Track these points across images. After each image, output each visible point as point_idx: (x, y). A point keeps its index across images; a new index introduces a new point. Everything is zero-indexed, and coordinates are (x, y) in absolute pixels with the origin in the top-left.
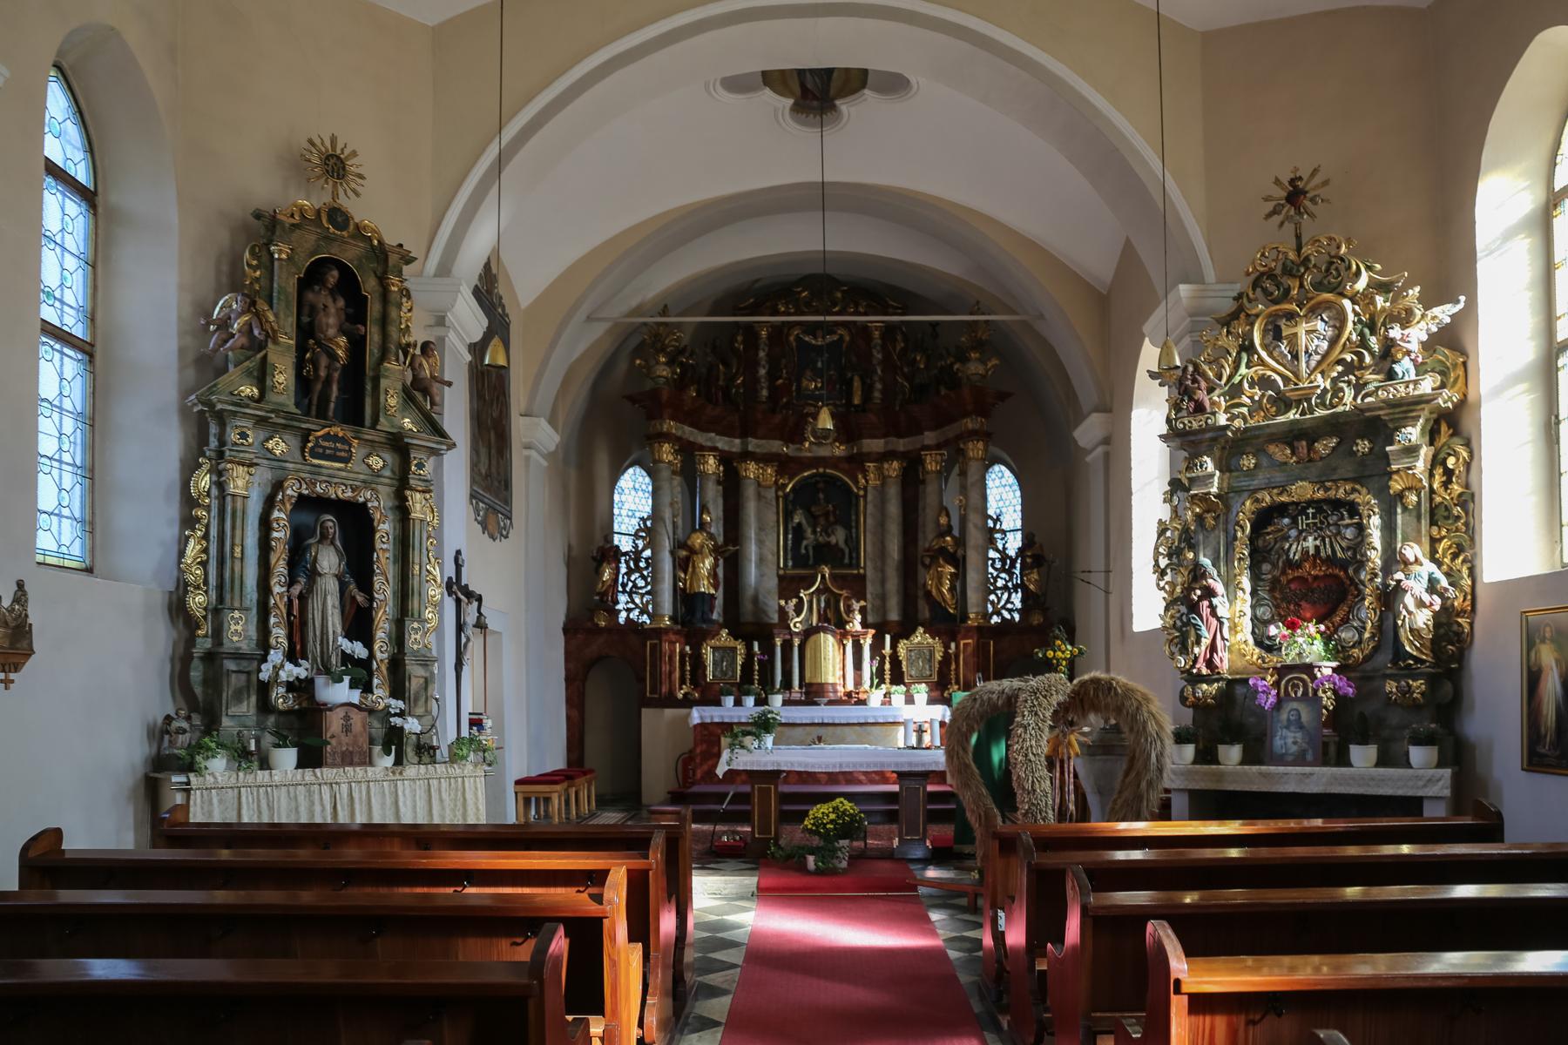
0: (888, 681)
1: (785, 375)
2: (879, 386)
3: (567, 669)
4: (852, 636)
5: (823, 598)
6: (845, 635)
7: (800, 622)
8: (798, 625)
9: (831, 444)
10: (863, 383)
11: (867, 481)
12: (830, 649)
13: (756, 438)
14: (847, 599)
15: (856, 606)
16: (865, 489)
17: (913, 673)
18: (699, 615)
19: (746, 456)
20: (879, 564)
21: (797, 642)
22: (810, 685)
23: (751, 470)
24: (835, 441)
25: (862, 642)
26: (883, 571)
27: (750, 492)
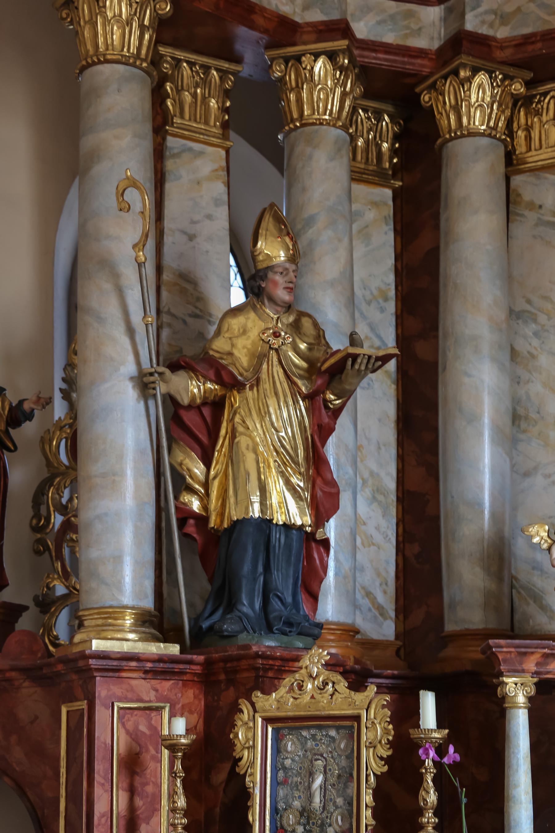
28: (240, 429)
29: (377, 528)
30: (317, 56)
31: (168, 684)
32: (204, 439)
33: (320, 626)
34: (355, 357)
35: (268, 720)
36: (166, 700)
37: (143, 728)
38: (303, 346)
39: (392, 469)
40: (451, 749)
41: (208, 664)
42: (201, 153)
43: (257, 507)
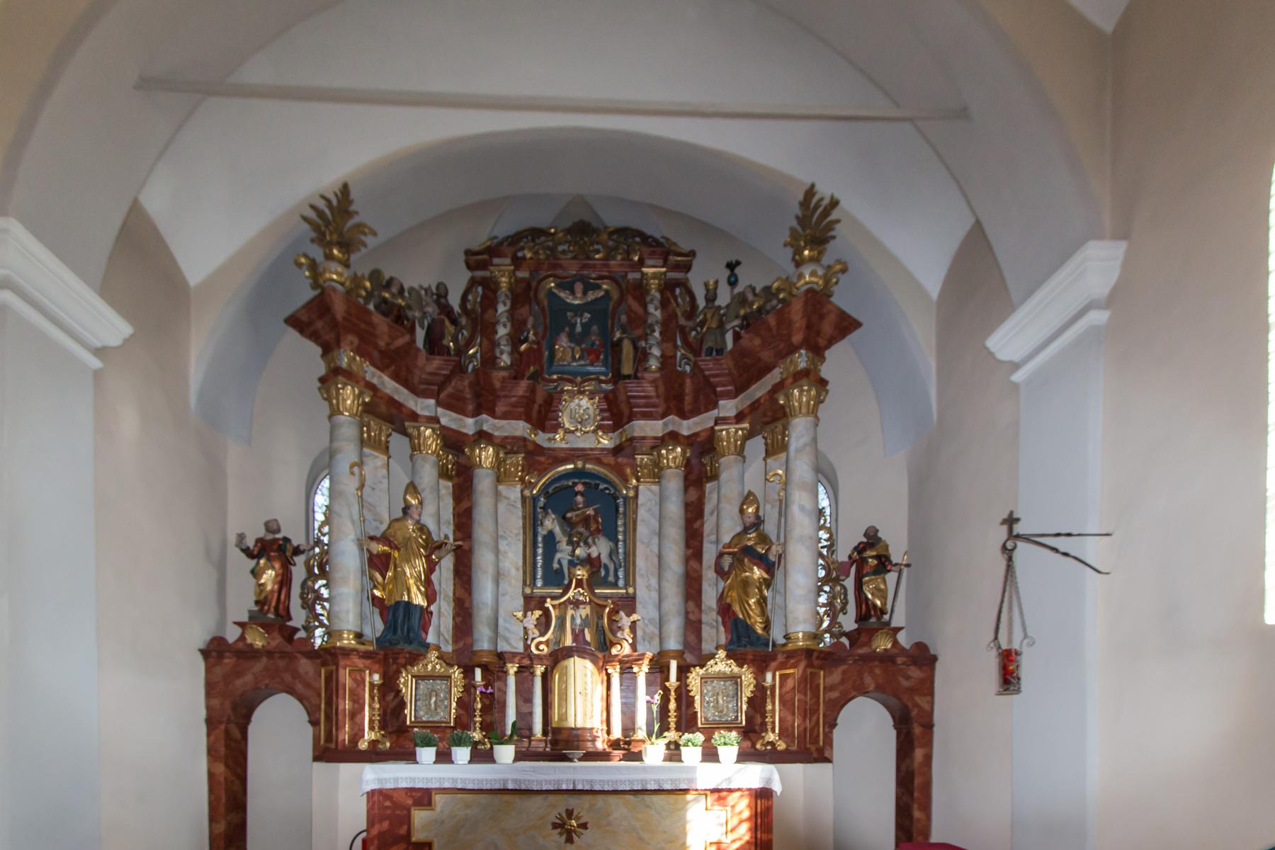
0: (673, 725)
1: (531, 337)
2: (656, 352)
3: (208, 708)
4: (621, 662)
6: (609, 659)
7: (547, 643)
10: (636, 348)
11: (638, 480)
16: (636, 489)
19: (483, 437)
22: (558, 731)
27: (484, 482)
29: (446, 610)
33: (429, 644)
34: (446, 544)
35: (413, 676)
36: (368, 668)
37: (358, 678)
38: (424, 537)
39: (452, 588)
40: (490, 688)
42: (376, 457)
43: (406, 597)
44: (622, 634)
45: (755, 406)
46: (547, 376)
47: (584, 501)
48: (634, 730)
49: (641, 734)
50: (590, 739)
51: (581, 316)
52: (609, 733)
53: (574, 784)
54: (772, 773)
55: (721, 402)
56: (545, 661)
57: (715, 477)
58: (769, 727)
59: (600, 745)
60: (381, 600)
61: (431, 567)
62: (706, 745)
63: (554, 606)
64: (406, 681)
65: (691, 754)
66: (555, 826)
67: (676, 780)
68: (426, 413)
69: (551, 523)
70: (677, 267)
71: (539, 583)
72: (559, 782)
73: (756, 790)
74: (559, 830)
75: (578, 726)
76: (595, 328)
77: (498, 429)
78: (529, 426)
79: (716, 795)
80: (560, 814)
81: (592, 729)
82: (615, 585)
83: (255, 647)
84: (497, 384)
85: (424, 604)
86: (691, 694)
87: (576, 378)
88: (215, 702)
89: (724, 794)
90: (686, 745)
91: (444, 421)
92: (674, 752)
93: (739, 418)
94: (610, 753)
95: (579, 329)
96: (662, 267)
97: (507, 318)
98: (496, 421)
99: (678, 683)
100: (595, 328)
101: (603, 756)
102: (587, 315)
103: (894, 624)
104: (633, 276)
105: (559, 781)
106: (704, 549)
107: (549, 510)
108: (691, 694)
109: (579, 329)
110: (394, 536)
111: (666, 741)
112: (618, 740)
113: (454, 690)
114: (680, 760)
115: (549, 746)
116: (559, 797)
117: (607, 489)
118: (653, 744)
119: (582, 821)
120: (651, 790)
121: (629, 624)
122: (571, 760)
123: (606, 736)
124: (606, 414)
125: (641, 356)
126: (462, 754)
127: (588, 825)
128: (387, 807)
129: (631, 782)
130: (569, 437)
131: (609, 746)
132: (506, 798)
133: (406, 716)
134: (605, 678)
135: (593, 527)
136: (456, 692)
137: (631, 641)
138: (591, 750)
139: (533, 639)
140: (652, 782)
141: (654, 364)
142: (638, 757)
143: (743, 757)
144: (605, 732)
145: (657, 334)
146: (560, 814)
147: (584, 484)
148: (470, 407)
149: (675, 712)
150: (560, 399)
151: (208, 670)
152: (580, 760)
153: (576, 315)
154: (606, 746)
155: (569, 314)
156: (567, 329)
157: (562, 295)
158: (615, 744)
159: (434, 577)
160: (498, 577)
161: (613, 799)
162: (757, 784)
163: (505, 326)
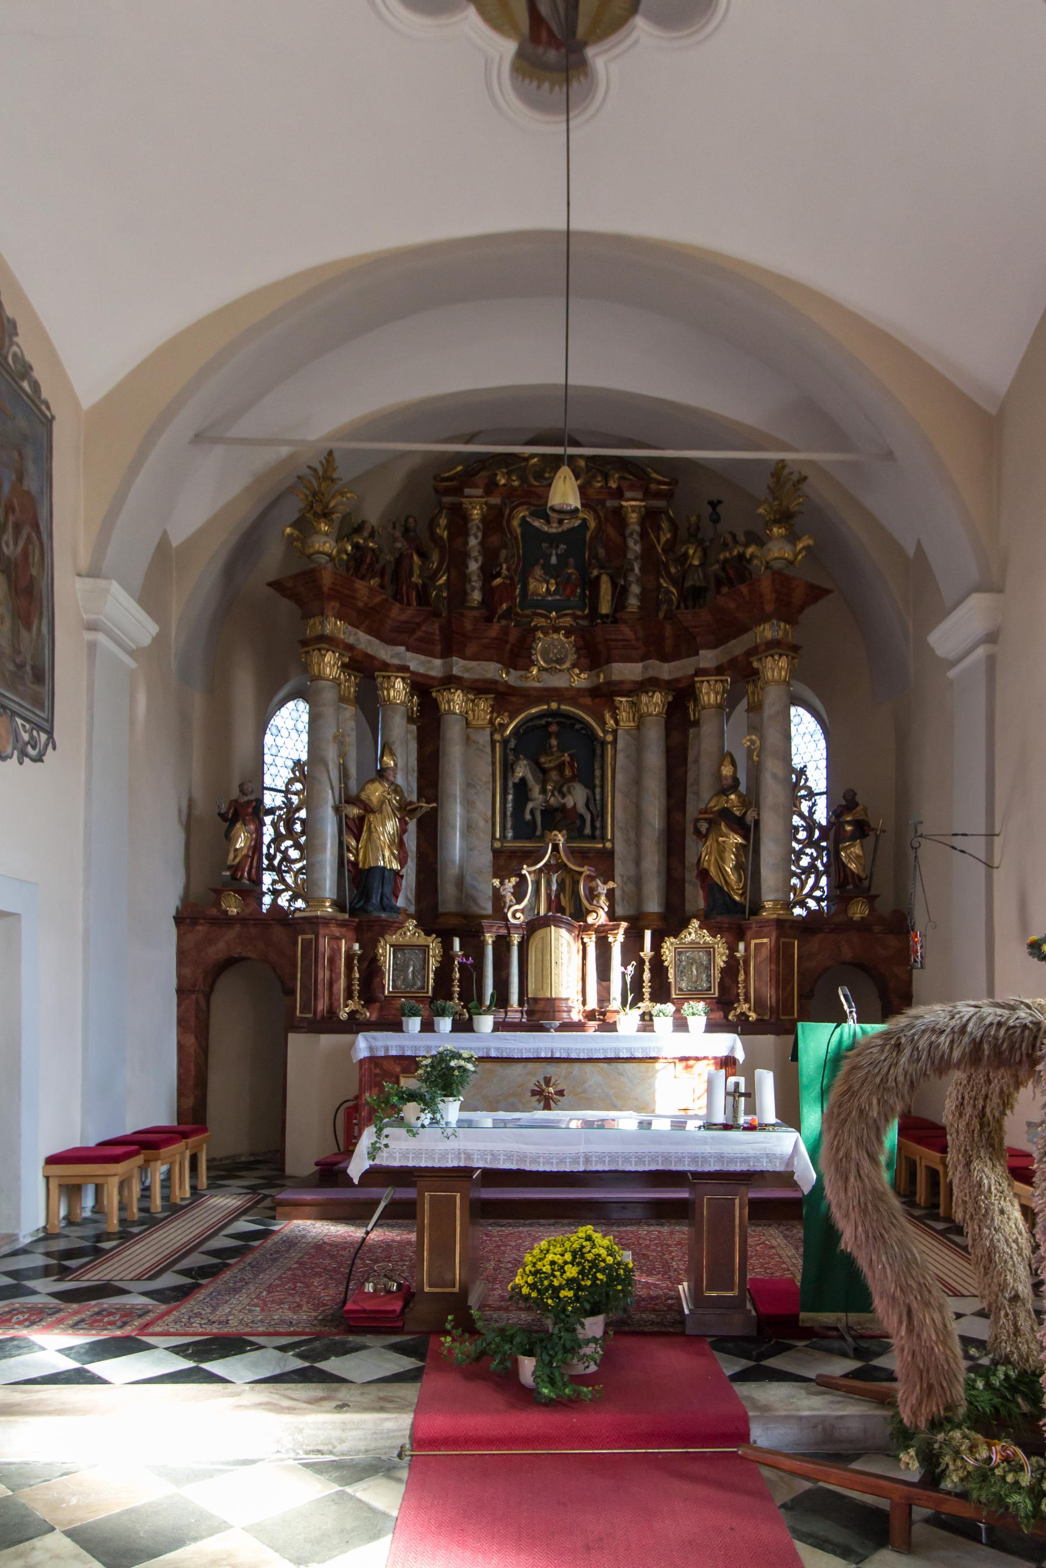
0: (647, 996)
1: (504, 572)
2: (635, 589)
3: (179, 976)
4: (597, 931)
5: (554, 879)
6: (587, 928)
7: (522, 911)
8: (518, 915)
9: (568, 670)
10: (614, 585)
11: (617, 722)
12: (564, 949)
13: (464, 659)
14: (590, 878)
15: (602, 889)
16: (615, 732)
17: (684, 985)
18: (375, 900)
19: (450, 681)
20: (632, 835)
21: (516, 939)
22: (536, 1000)
23: (456, 701)
24: (574, 666)
25: (611, 939)
26: (638, 845)
27: (453, 733)
28: (373, 830)
30: (397, 677)
31: (344, 929)
32: (356, 832)
41: (360, 921)
43: (382, 862)
44: (598, 902)
45: (733, 663)
46: (519, 610)
47: (558, 744)
48: (609, 1001)
49: (615, 1004)
50: (566, 1009)
51: (557, 547)
52: (584, 1003)
53: (552, 1051)
54: (735, 1041)
55: (701, 652)
56: (521, 931)
57: (696, 723)
58: (741, 998)
59: (576, 1016)
60: (355, 864)
61: (403, 830)
62: (677, 1016)
63: (530, 873)
64: (385, 949)
65: (664, 1022)
66: (534, 1093)
67: (646, 1048)
68: (396, 661)
69: (522, 770)
70: (658, 495)
71: (510, 834)
72: (537, 1050)
73: (721, 1058)
74: (538, 1097)
75: (553, 996)
76: (571, 561)
77: (467, 670)
78: (499, 666)
79: (684, 1064)
80: (538, 1082)
81: (567, 999)
82: (592, 837)
83: (230, 913)
84: (468, 626)
85: (396, 866)
86: (666, 964)
87: (551, 613)
88: (187, 971)
89: (691, 1062)
90: (658, 1015)
91: (413, 666)
92: (647, 1022)
93: (719, 670)
94: (585, 1023)
95: (554, 560)
96: (641, 500)
97: (479, 552)
98: (466, 662)
99: (653, 953)
100: (571, 561)
101: (579, 1027)
102: (563, 547)
103: (873, 892)
104: (609, 503)
105: (538, 1049)
106: (688, 800)
107: (521, 756)
108: (666, 964)
109: (554, 560)
110: (370, 800)
111: (641, 1012)
112: (593, 1011)
113: (431, 960)
114: (653, 1031)
115: (525, 1016)
116: (538, 1065)
117: (582, 729)
118: (627, 1014)
119: (560, 1088)
120: (623, 1058)
121: (605, 891)
122: (548, 1030)
123: (581, 1006)
124: (583, 652)
125: (620, 594)
126: (445, 1024)
127: (565, 1093)
128: (376, 1075)
129: (605, 1050)
130: (545, 675)
131: (584, 1018)
132: (488, 1066)
133: (384, 986)
134: (581, 947)
135: (568, 772)
136: (433, 964)
137: (606, 909)
138: (567, 1020)
139: (510, 906)
140: (625, 1051)
141: (633, 602)
142: (612, 1027)
143: (712, 1027)
144: (580, 1002)
145: (637, 570)
146: (538, 1082)
147: (558, 724)
148: (438, 648)
149: (650, 982)
150: (534, 637)
151: (180, 937)
152: (556, 1030)
153: (551, 546)
154: (581, 1018)
155: (544, 545)
156: (542, 561)
157: (536, 524)
158: (590, 1016)
159: (405, 837)
160: (469, 828)
161: (588, 1067)
162: (723, 1053)
163: (476, 561)
